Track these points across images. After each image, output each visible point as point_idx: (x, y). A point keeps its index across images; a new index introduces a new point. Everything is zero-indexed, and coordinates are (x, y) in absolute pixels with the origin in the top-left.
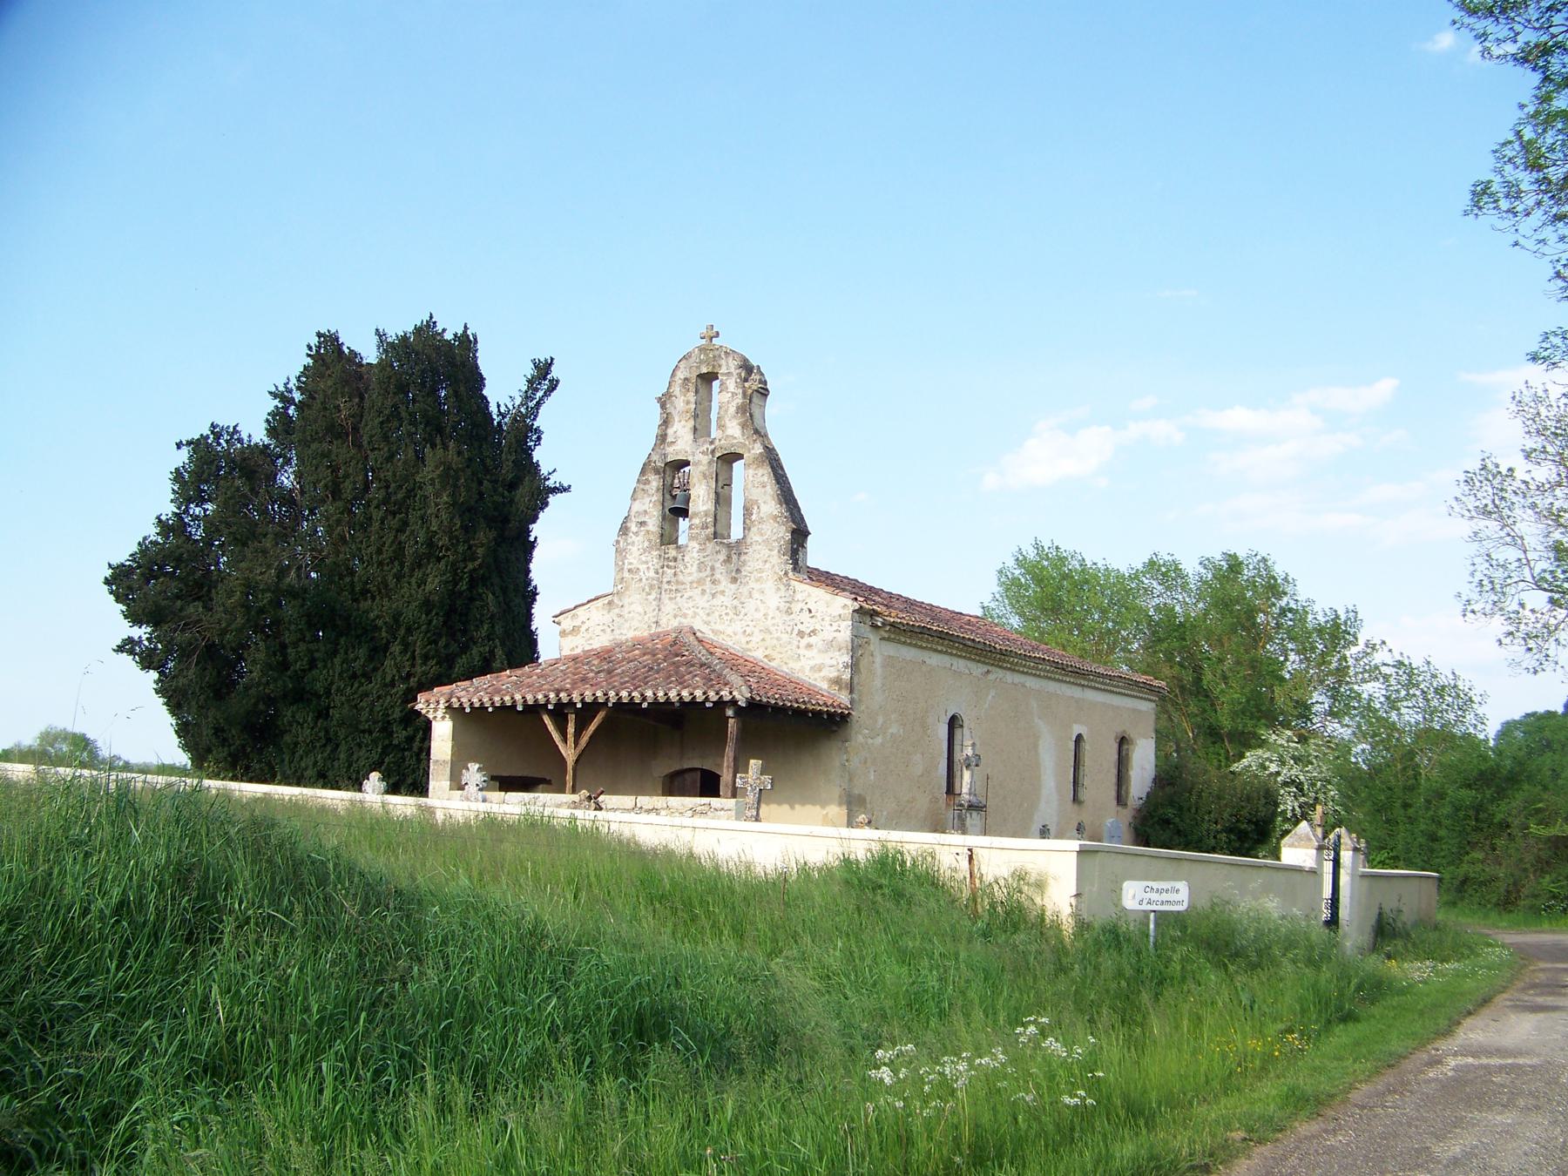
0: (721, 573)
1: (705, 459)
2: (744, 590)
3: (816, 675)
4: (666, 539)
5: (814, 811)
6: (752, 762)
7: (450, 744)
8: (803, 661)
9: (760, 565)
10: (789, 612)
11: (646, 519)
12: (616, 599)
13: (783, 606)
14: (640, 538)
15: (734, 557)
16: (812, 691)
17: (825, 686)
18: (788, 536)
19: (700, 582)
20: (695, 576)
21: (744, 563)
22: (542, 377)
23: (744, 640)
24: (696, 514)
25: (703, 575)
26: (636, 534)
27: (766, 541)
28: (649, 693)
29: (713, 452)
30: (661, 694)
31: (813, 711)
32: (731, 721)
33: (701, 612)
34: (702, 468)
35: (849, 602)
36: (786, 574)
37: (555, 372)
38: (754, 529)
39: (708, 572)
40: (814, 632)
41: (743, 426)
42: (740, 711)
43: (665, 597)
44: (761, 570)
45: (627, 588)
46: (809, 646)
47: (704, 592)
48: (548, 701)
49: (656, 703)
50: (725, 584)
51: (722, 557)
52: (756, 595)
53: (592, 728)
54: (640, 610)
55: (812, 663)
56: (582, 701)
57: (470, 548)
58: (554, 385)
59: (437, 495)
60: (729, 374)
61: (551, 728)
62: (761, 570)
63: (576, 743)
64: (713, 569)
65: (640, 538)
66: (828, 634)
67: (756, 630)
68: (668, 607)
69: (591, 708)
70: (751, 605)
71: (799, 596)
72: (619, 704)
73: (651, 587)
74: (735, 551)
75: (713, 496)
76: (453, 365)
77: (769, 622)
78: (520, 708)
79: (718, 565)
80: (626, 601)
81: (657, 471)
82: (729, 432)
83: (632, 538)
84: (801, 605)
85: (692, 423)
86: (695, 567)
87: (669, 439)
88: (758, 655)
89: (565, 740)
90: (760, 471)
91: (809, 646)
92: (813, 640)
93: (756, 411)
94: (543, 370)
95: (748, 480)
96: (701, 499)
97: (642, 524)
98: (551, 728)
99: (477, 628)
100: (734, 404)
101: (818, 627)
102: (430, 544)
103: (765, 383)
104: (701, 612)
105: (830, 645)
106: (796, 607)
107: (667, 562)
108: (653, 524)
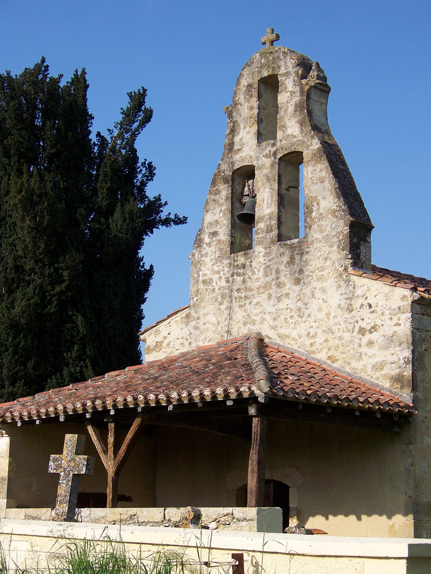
0: (286, 278)
1: (268, 162)
2: (307, 290)
3: (378, 374)
4: (236, 247)
5: (378, 521)
6: (68, 436)
7: (7, 461)
8: (365, 360)
9: (319, 263)
10: (350, 309)
11: (217, 229)
12: (192, 312)
13: (344, 303)
14: (213, 249)
15: (297, 257)
16: (371, 389)
17: (387, 384)
18: (346, 230)
19: (266, 286)
20: (262, 281)
21: (306, 263)
22: (138, 111)
23: (308, 342)
24: (261, 219)
25: (268, 279)
26: (209, 245)
27: (327, 238)
28: (174, 395)
29: (275, 153)
30: (185, 394)
31: (360, 409)
32: (255, 420)
33: (268, 317)
34: (265, 171)
35: (408, 293)
36: (346, 269)
37: (148, 103)
38: (315, 227)
39: (274, 276)
40: (374, 328)
41: (302, 124)
42: (263, 410)
43: (235, 305)
44: (322, 269)
45: (202, 300)
46: (370, 343)
47: (270, 297)
48: (85, 410)
49: (180, 405)
50: (289, 286)
51: (286, 259)
52: (318, 294)
53: (129, 436)
54: (214, 320)
55: (374, 361)
56: (115, 406)
57: (56, 270)
58: (148, 116)
59: (23, 220)
60: (287, 74)
61: (94, 438)
62: (322, 269)
63: (115, 453)
64: (278, 272)
65: (213, 249)
66: (388, 328)
67: (320, 331)
68: (239, 315)
69: (125, 415)
70: (314, 305)
71: (359, 292)
72: (147, 408)
73: (223, 296)
74: (298, 252)
75: (275, 198)
76: (13, 89)
77: (332, 321)
78: (62, 419)
79: (282, 267)
80: (201, 312)
81: (225, 180)
82: (289, 131)
83: (206, 249)
84: (361, 301)
85: (255, 128)
86: (262, 271)
87: (236, 147)
88: (322, 356)
89: (106, 452)
90: (319, 167)
91: (370, 343)
92: (374, 336)
93: (316, 109)
94: (138, 100)
95: (316, 180)
96: (266, 202)
97: (214, 234)
98: (94, 438)
99: (69, 349)
100: (293, 103)
101: (379, 322)
102: (18, 268)
103: (325, 79)
104: (268, 317)
105: (391, 340)
106: (357, 303)
107: (237, 269)
108: (224, 234)
